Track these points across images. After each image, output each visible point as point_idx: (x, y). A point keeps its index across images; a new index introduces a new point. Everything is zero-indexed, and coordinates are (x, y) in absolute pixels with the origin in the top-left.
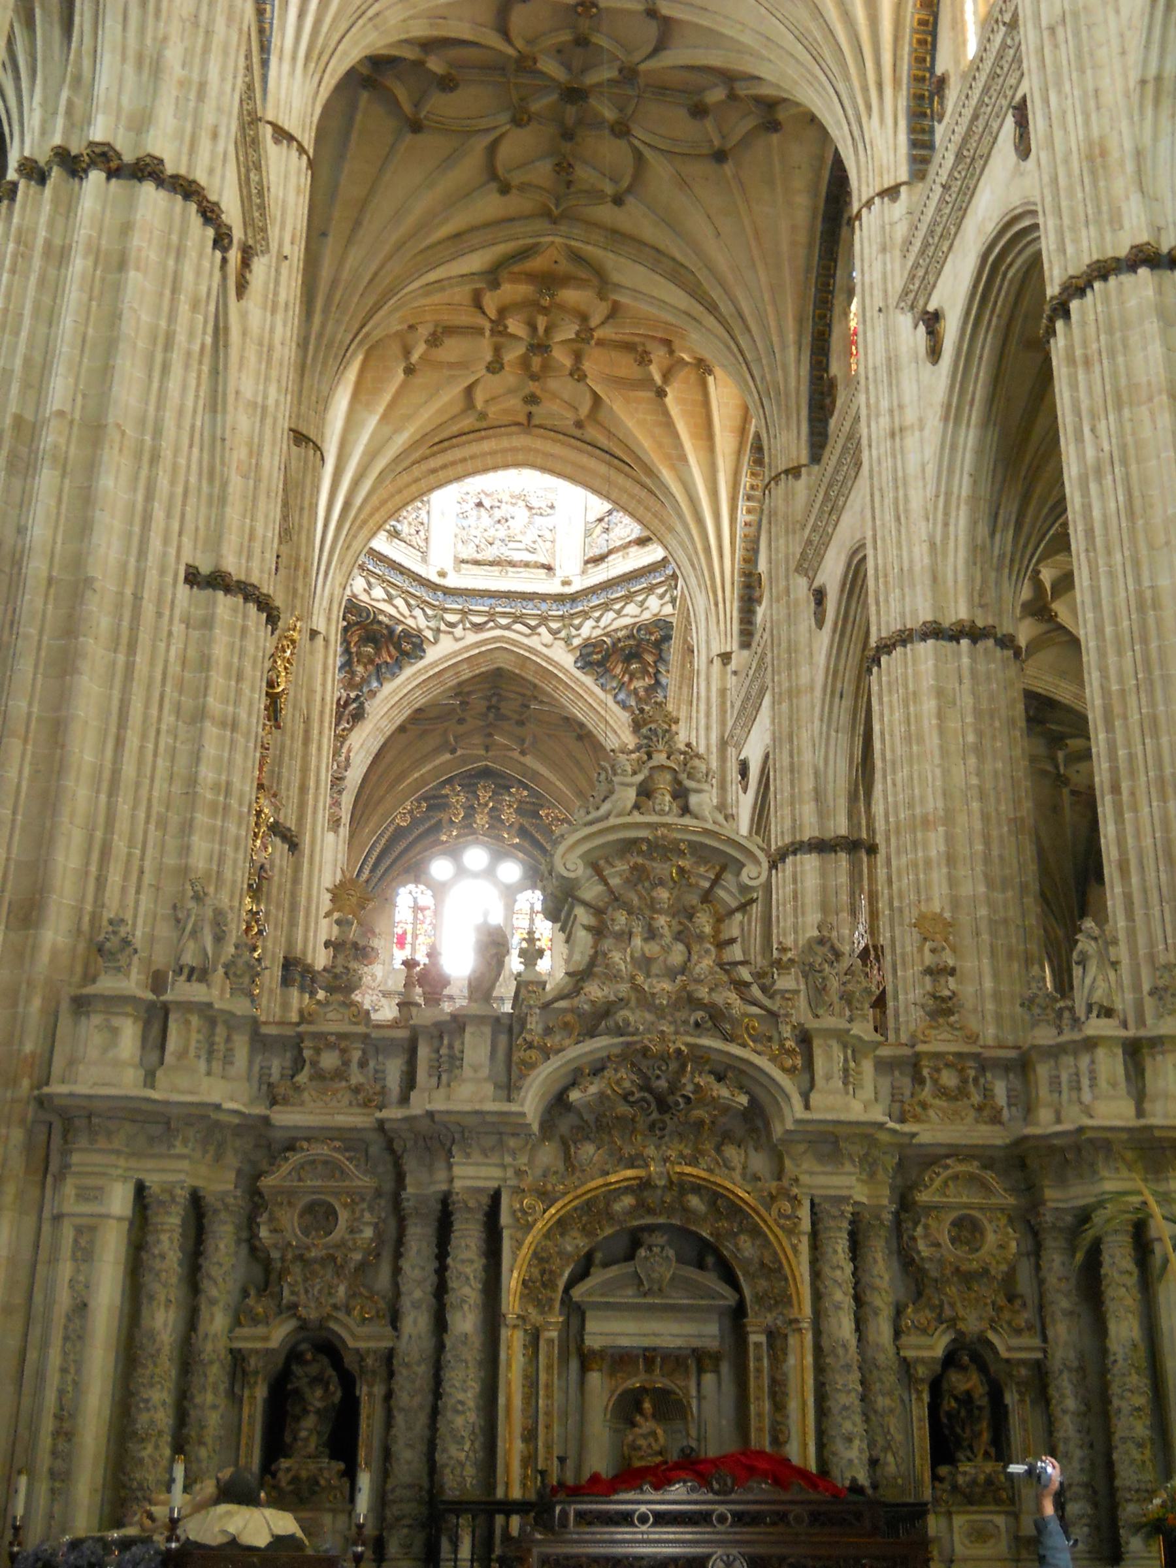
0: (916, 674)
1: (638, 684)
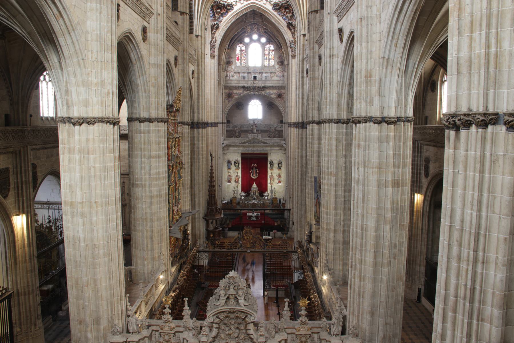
0: (332, 133)
1: (289, 15)
